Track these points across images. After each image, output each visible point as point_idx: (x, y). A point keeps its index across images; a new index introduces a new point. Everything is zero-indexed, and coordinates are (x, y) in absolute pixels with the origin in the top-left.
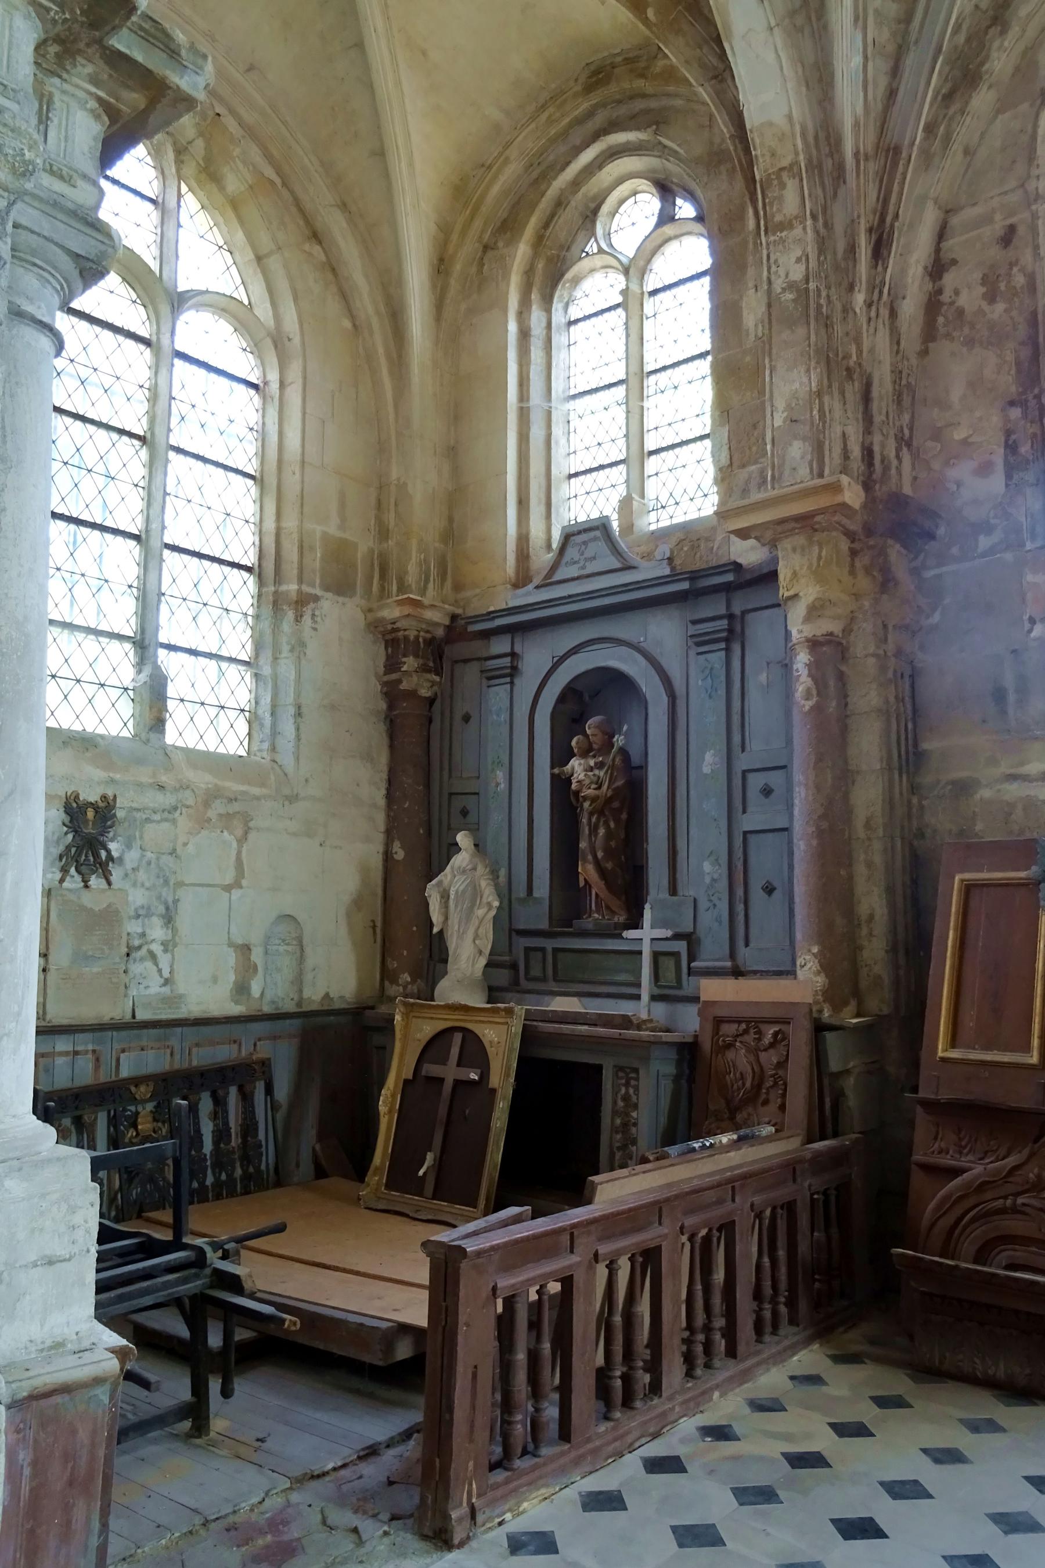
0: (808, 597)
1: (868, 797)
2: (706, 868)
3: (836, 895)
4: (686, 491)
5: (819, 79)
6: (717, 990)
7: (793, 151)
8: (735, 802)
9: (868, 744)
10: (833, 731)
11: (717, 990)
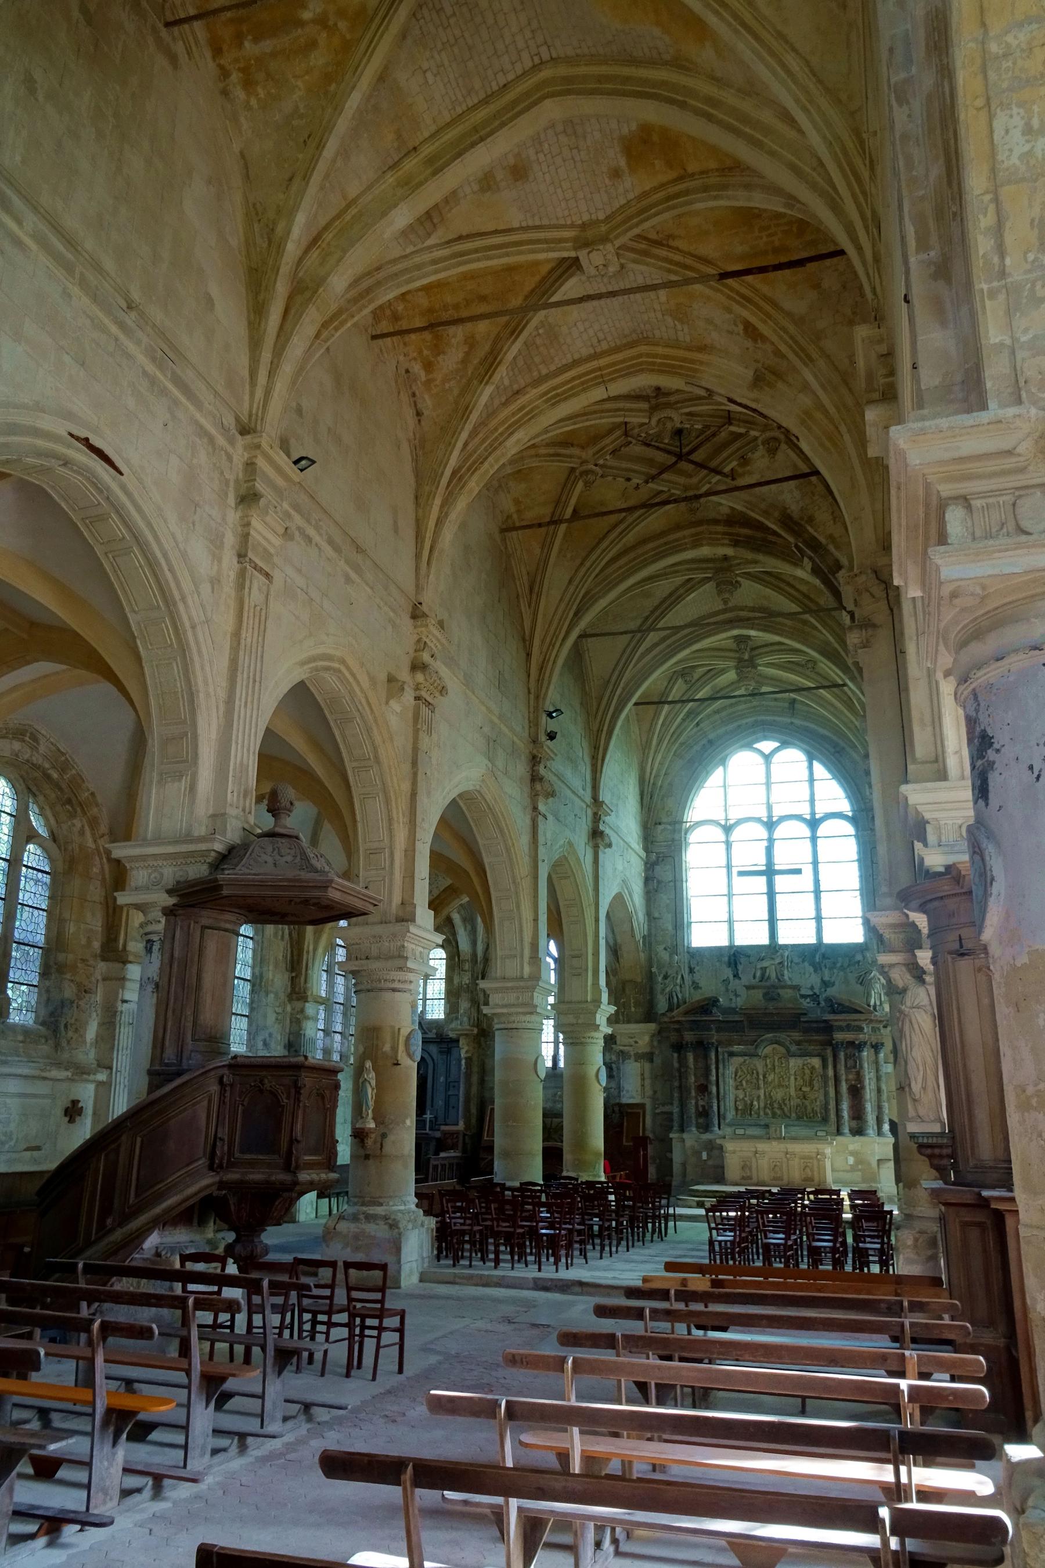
0: (464, 1050)
1: (474, 1090)
2: (440, 1103)
3: (467, 1109)
4: (437, 1011)
5: (474, 943)
6: (443, 1128)
7: (468, 957)
8: (447, 1089)
9: (475, 1079)
10: (468, 1075)
11: (443, 1128)
